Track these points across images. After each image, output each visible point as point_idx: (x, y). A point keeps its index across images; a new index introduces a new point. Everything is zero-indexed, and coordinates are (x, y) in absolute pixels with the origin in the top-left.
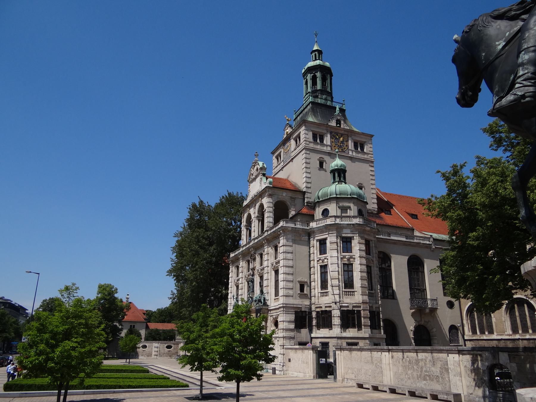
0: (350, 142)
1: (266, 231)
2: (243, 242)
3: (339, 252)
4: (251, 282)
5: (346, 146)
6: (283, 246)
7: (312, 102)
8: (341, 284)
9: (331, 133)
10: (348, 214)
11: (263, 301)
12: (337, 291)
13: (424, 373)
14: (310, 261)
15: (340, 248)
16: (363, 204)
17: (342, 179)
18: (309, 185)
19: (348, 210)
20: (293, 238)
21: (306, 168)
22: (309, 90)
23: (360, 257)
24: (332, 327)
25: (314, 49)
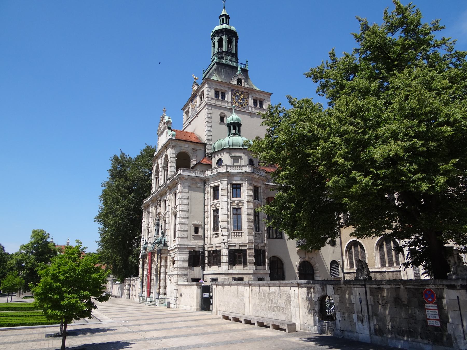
0: (250, 99)
2: (153, 190)
3: (229, 197)
5: (246, 102)
6: (180, 192)
7: (217, 63)
8: (229, 226)
9: (232, 90)
10: (239, 164)
11: (163, 242)
12: (225, 233)
14: (205, 206)
15: (230, 194)
18: (210, 138)
19: (240, 160)
20: (190, 185)
21: (208, 122)
22: (216, 51)
23: (248, 202)
24: (220, 265)
25: (222, 14)
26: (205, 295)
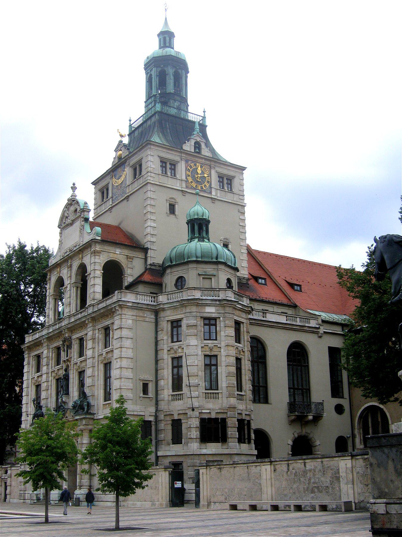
1: (90, 306)
7: (160, 113)
9: (187, 161)
13: (312, 485)
26: (176, 483)
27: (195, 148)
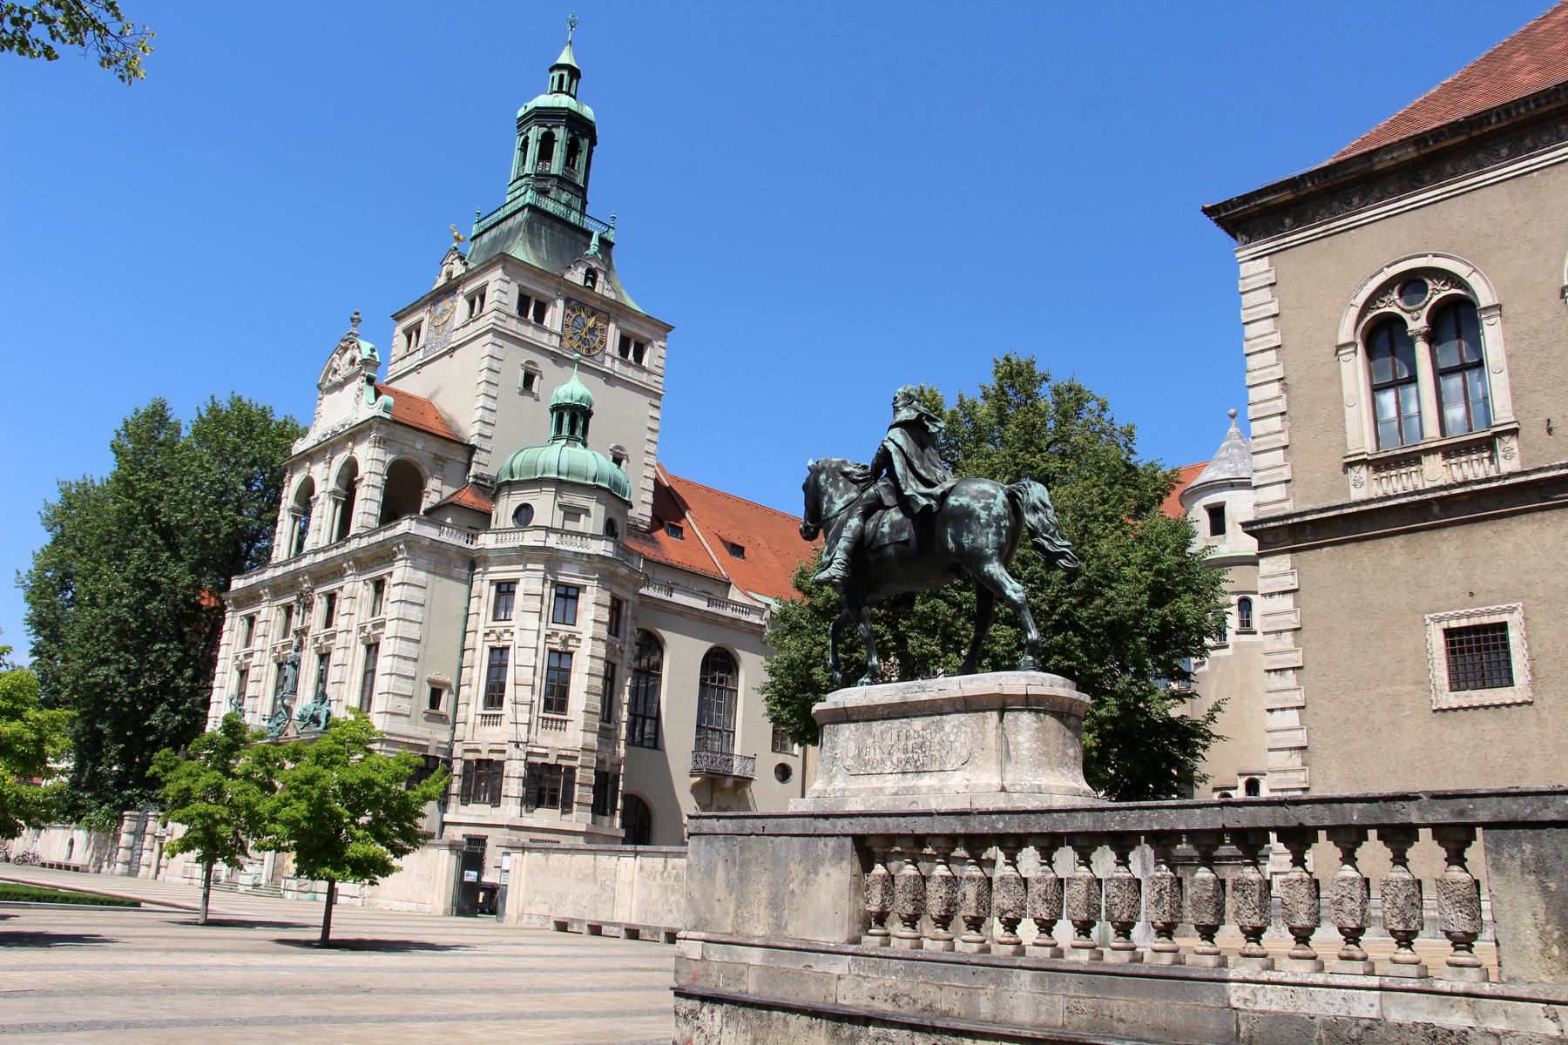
1: (354, 536)
4: (286, 667)
7: (532, 208)
8: (536, 698)
9: (567, 301)
11: (323, 720)
16: (619, 505)
17: (578, 433)
18: (488, 431)
25: (560, 61)
27: (586, 279)
